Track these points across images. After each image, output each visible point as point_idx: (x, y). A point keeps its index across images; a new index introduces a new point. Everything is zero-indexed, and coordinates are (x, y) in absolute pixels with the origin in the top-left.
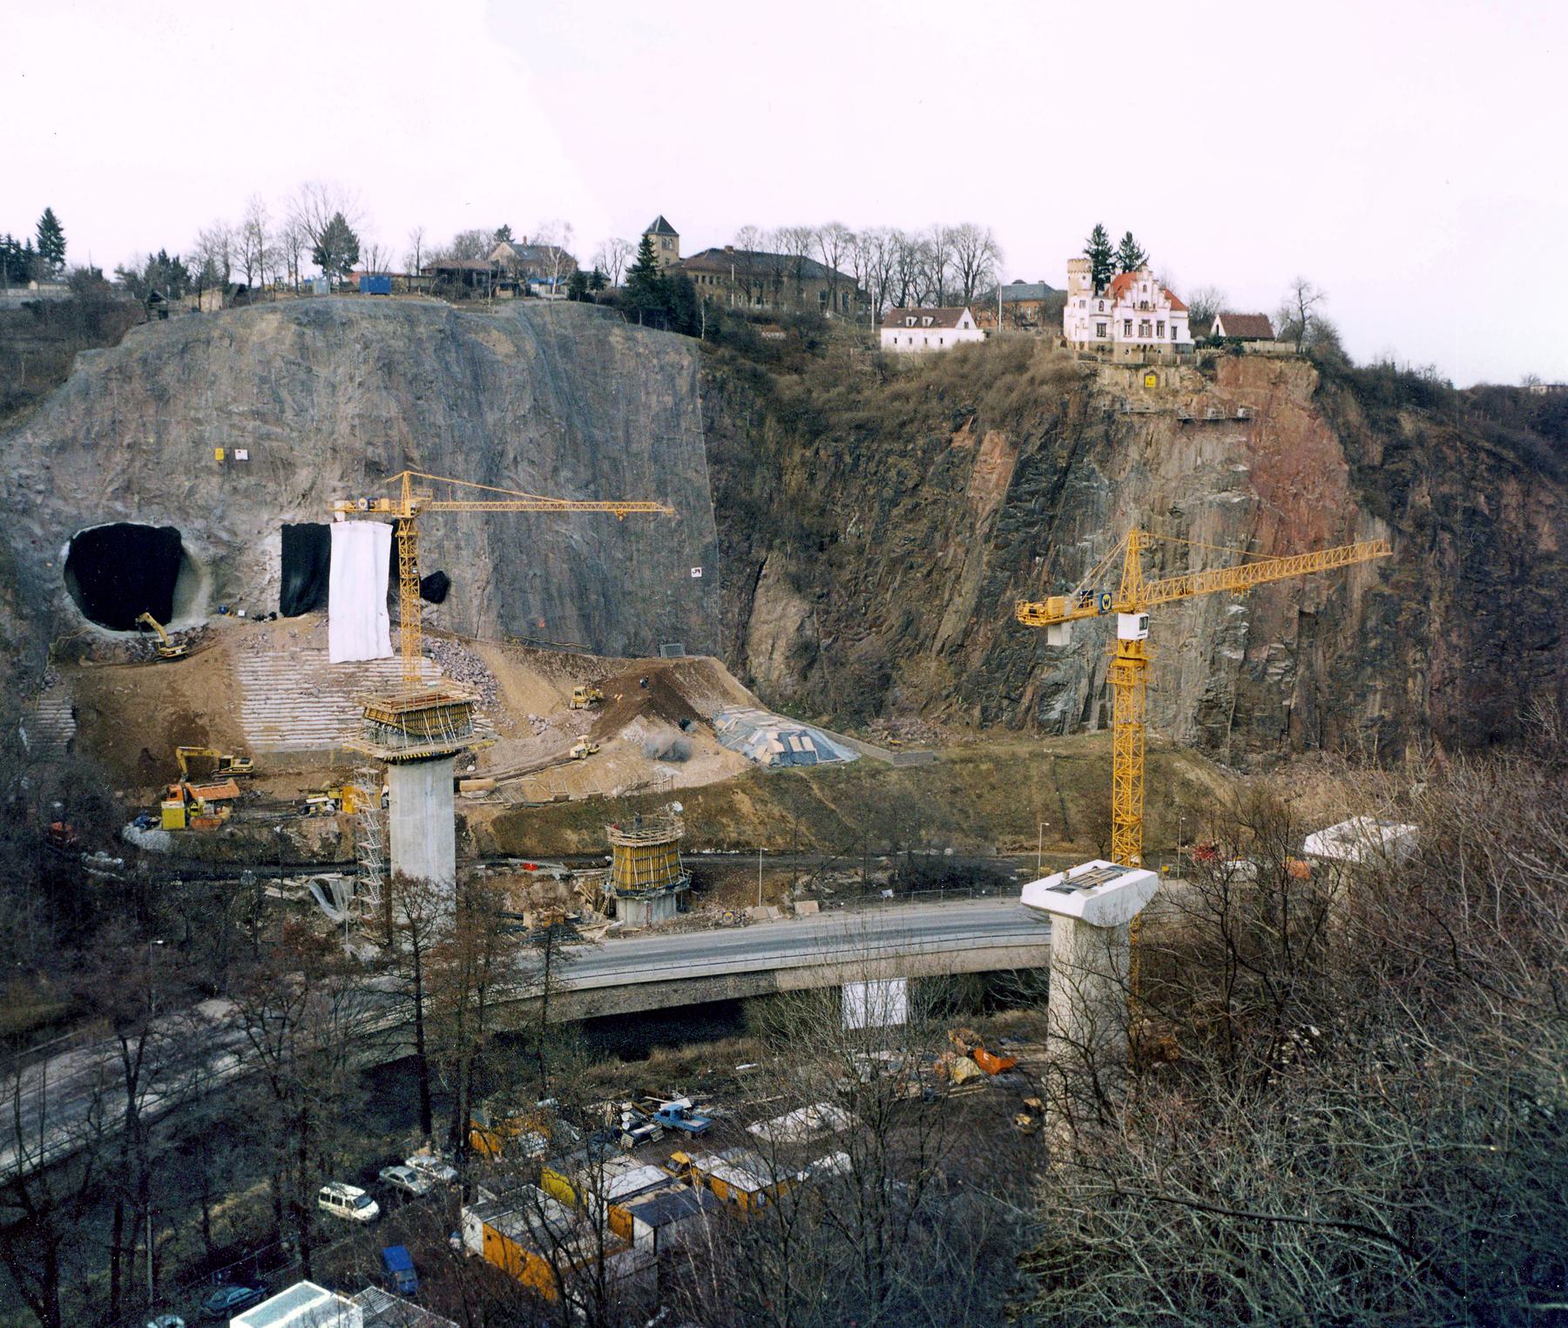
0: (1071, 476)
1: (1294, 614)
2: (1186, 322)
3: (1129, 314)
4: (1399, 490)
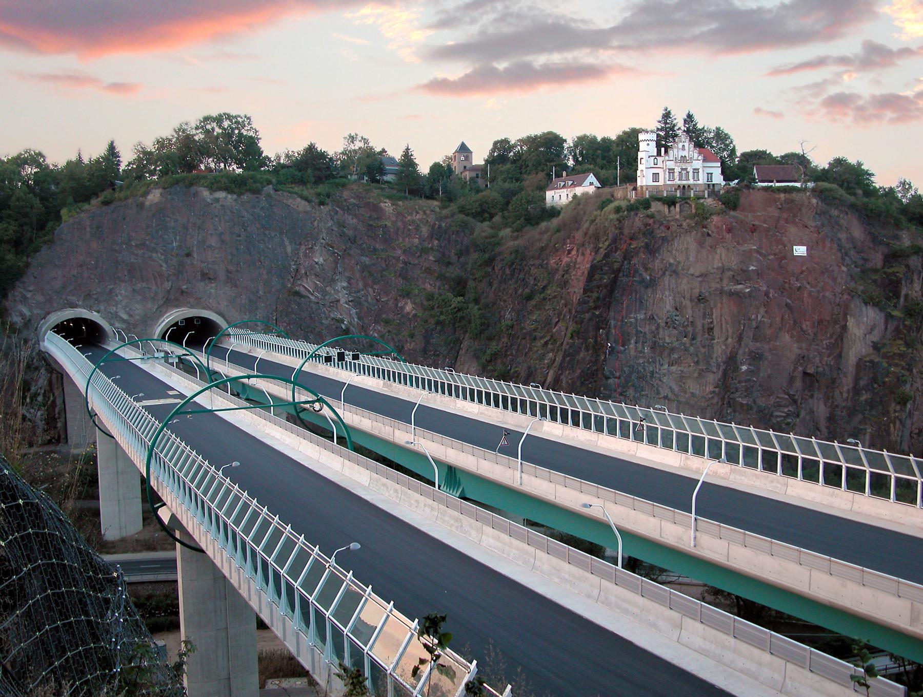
0: (621, 275)
1: (798, 374)
2: (720, 170)
3: (671, 165)
4: (892, 288)
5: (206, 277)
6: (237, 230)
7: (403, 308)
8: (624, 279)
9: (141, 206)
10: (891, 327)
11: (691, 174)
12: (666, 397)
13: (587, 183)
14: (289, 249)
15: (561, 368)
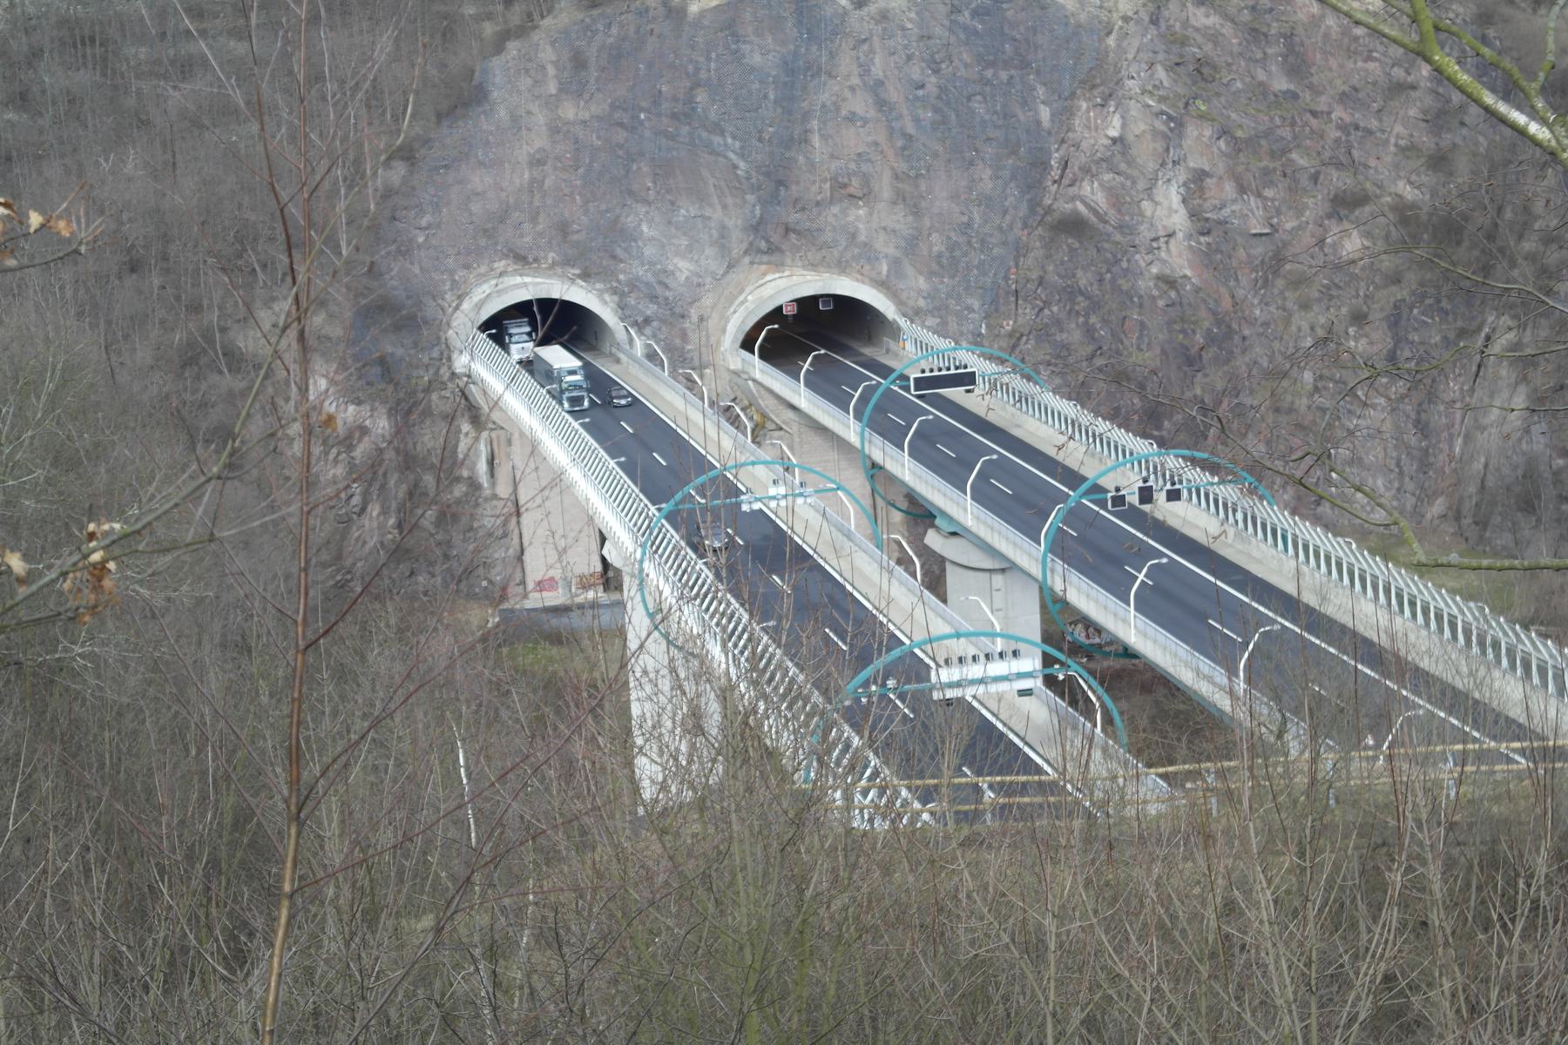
5: (841, 190)
6: (916, 72)
14: (1045, 113)
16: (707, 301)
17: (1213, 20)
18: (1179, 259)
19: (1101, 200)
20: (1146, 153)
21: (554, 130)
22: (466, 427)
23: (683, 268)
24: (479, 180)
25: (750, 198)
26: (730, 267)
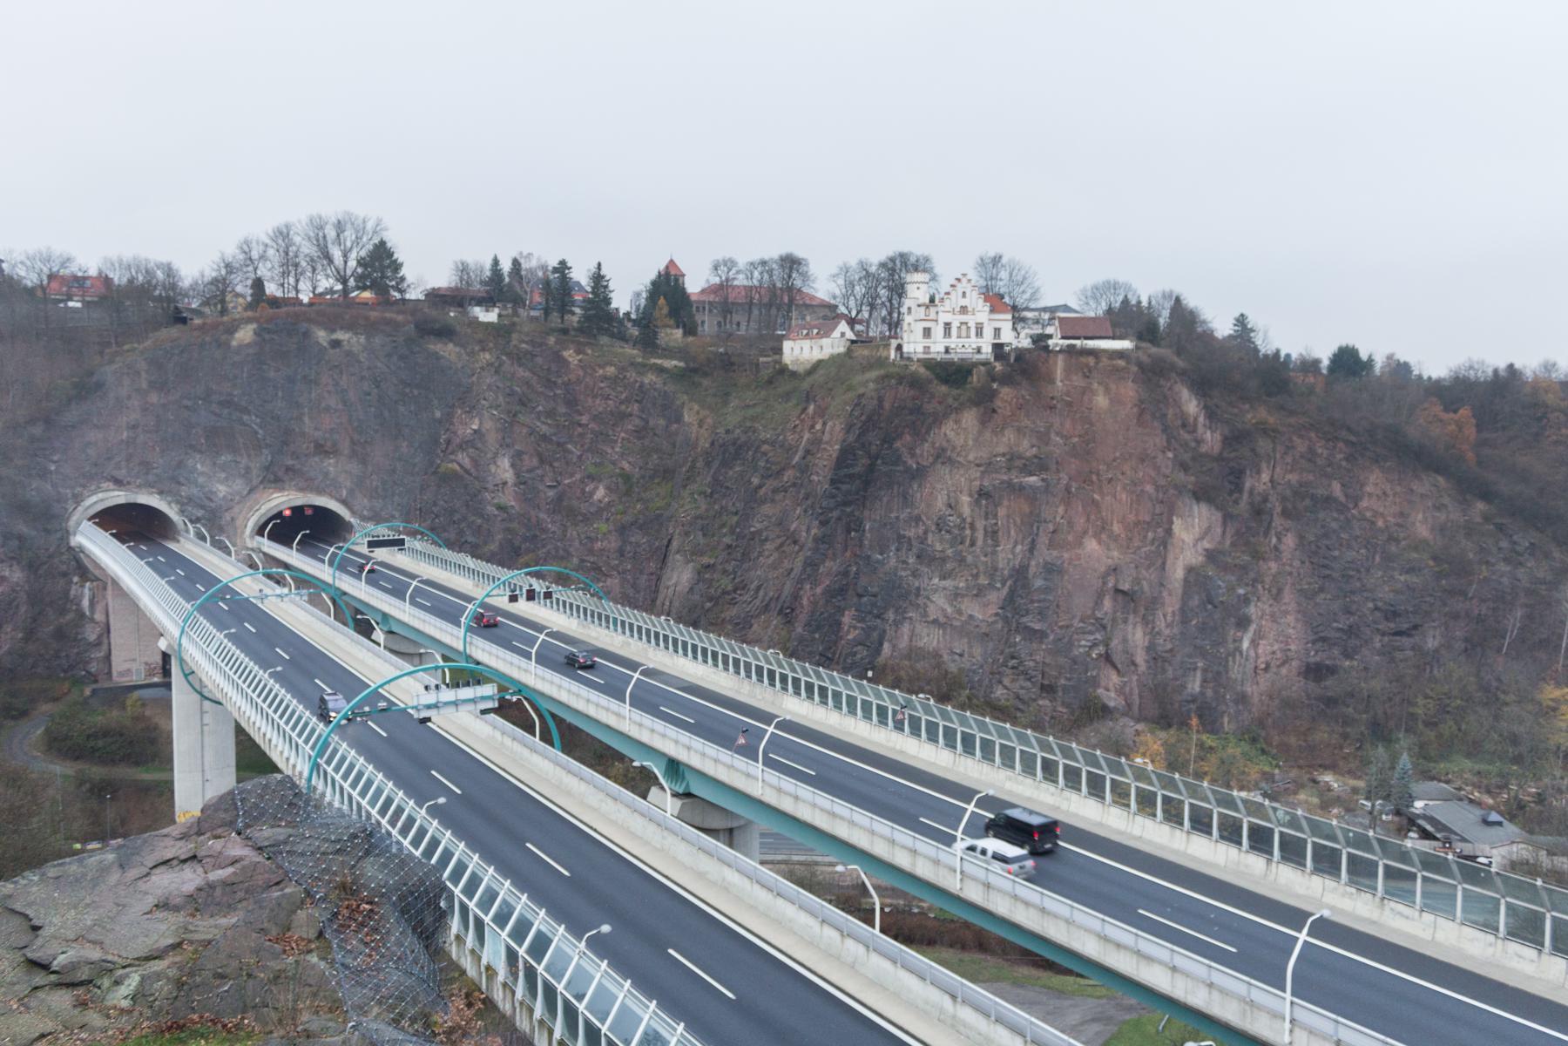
2: (1010, 324)
5: (321, 449)
7: (592, 493)
8: (884, 469)
9: (227, 345)
10: (1230, 531)
11: (973, 331)
12: (935, 621)
13: (836, 334)
15: (800, 581)
16: (236, 509)
17: (527, 374)
18: (508, 498)
19: (467, 462)
20: (492, 439)
21: (144, 410)
22: (76, 579)
23: (222, 490)
24: (93, 435)
25: (266, 451)
26: (250, 492)
